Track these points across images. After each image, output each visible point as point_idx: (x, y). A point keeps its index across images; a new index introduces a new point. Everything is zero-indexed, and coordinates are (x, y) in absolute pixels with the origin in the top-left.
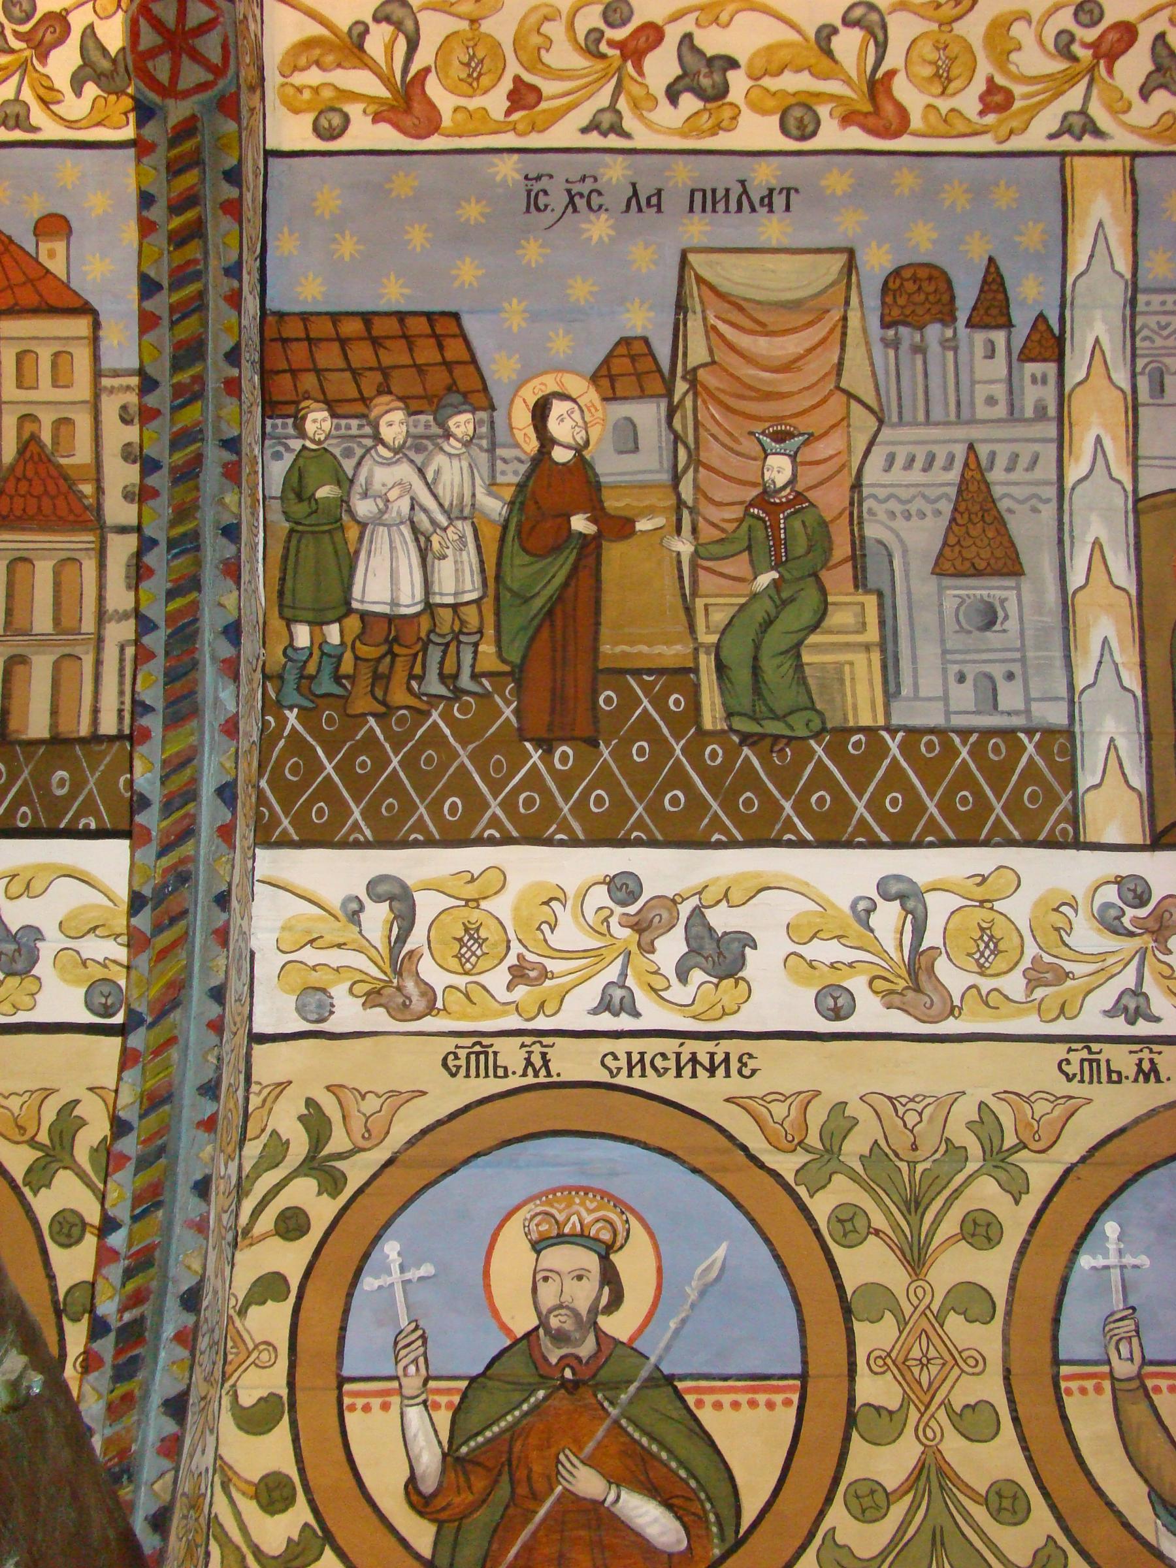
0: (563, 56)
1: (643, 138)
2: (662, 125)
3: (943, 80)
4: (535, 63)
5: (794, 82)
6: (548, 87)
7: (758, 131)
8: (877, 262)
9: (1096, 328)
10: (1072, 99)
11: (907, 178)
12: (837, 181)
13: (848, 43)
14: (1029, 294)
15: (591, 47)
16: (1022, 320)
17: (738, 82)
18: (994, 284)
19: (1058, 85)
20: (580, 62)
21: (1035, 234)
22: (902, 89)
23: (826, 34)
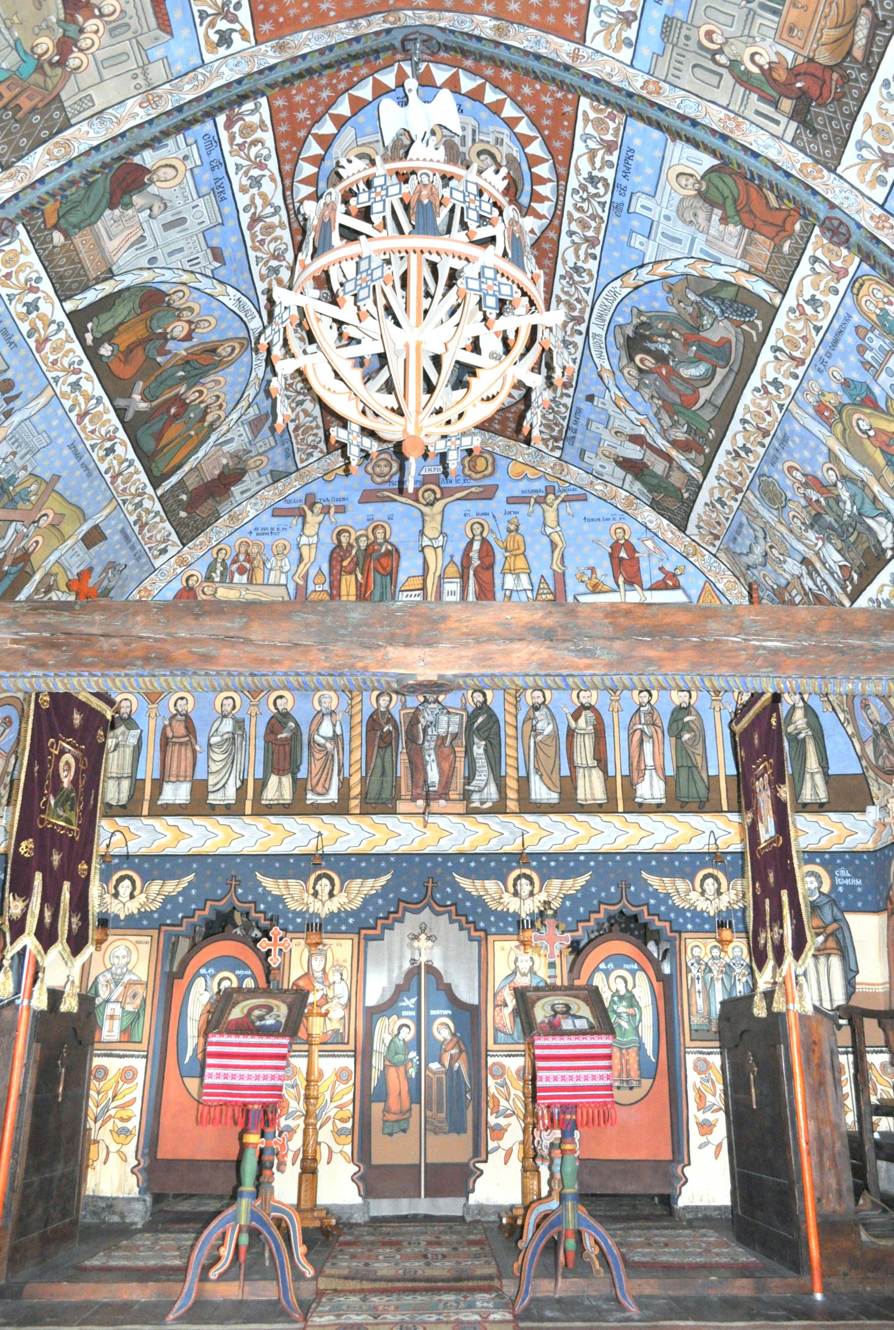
0: (22, 277)
1: (11, 308)
2: (17, 308)
3: (54, 350)
4: (17, 273)
5: (40, 325)
6: (13, 279)
7: (25, 327)
8: (9, 375)
9: (16, 418)
10: (61, 374)
11: (31, 362)
12: (23, 352)
13: (54, 327)
14: (17, 403)
15: (27, 281)
16: (11, 405)
17: (35, 314)
18: (17, 396)
19: (64, 370)
20: (23, 281)
21: (30, 395)
22: (49, 345)
23: (54, 322)
